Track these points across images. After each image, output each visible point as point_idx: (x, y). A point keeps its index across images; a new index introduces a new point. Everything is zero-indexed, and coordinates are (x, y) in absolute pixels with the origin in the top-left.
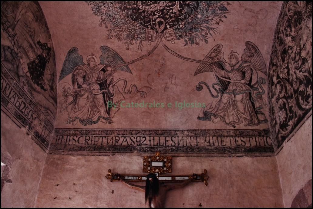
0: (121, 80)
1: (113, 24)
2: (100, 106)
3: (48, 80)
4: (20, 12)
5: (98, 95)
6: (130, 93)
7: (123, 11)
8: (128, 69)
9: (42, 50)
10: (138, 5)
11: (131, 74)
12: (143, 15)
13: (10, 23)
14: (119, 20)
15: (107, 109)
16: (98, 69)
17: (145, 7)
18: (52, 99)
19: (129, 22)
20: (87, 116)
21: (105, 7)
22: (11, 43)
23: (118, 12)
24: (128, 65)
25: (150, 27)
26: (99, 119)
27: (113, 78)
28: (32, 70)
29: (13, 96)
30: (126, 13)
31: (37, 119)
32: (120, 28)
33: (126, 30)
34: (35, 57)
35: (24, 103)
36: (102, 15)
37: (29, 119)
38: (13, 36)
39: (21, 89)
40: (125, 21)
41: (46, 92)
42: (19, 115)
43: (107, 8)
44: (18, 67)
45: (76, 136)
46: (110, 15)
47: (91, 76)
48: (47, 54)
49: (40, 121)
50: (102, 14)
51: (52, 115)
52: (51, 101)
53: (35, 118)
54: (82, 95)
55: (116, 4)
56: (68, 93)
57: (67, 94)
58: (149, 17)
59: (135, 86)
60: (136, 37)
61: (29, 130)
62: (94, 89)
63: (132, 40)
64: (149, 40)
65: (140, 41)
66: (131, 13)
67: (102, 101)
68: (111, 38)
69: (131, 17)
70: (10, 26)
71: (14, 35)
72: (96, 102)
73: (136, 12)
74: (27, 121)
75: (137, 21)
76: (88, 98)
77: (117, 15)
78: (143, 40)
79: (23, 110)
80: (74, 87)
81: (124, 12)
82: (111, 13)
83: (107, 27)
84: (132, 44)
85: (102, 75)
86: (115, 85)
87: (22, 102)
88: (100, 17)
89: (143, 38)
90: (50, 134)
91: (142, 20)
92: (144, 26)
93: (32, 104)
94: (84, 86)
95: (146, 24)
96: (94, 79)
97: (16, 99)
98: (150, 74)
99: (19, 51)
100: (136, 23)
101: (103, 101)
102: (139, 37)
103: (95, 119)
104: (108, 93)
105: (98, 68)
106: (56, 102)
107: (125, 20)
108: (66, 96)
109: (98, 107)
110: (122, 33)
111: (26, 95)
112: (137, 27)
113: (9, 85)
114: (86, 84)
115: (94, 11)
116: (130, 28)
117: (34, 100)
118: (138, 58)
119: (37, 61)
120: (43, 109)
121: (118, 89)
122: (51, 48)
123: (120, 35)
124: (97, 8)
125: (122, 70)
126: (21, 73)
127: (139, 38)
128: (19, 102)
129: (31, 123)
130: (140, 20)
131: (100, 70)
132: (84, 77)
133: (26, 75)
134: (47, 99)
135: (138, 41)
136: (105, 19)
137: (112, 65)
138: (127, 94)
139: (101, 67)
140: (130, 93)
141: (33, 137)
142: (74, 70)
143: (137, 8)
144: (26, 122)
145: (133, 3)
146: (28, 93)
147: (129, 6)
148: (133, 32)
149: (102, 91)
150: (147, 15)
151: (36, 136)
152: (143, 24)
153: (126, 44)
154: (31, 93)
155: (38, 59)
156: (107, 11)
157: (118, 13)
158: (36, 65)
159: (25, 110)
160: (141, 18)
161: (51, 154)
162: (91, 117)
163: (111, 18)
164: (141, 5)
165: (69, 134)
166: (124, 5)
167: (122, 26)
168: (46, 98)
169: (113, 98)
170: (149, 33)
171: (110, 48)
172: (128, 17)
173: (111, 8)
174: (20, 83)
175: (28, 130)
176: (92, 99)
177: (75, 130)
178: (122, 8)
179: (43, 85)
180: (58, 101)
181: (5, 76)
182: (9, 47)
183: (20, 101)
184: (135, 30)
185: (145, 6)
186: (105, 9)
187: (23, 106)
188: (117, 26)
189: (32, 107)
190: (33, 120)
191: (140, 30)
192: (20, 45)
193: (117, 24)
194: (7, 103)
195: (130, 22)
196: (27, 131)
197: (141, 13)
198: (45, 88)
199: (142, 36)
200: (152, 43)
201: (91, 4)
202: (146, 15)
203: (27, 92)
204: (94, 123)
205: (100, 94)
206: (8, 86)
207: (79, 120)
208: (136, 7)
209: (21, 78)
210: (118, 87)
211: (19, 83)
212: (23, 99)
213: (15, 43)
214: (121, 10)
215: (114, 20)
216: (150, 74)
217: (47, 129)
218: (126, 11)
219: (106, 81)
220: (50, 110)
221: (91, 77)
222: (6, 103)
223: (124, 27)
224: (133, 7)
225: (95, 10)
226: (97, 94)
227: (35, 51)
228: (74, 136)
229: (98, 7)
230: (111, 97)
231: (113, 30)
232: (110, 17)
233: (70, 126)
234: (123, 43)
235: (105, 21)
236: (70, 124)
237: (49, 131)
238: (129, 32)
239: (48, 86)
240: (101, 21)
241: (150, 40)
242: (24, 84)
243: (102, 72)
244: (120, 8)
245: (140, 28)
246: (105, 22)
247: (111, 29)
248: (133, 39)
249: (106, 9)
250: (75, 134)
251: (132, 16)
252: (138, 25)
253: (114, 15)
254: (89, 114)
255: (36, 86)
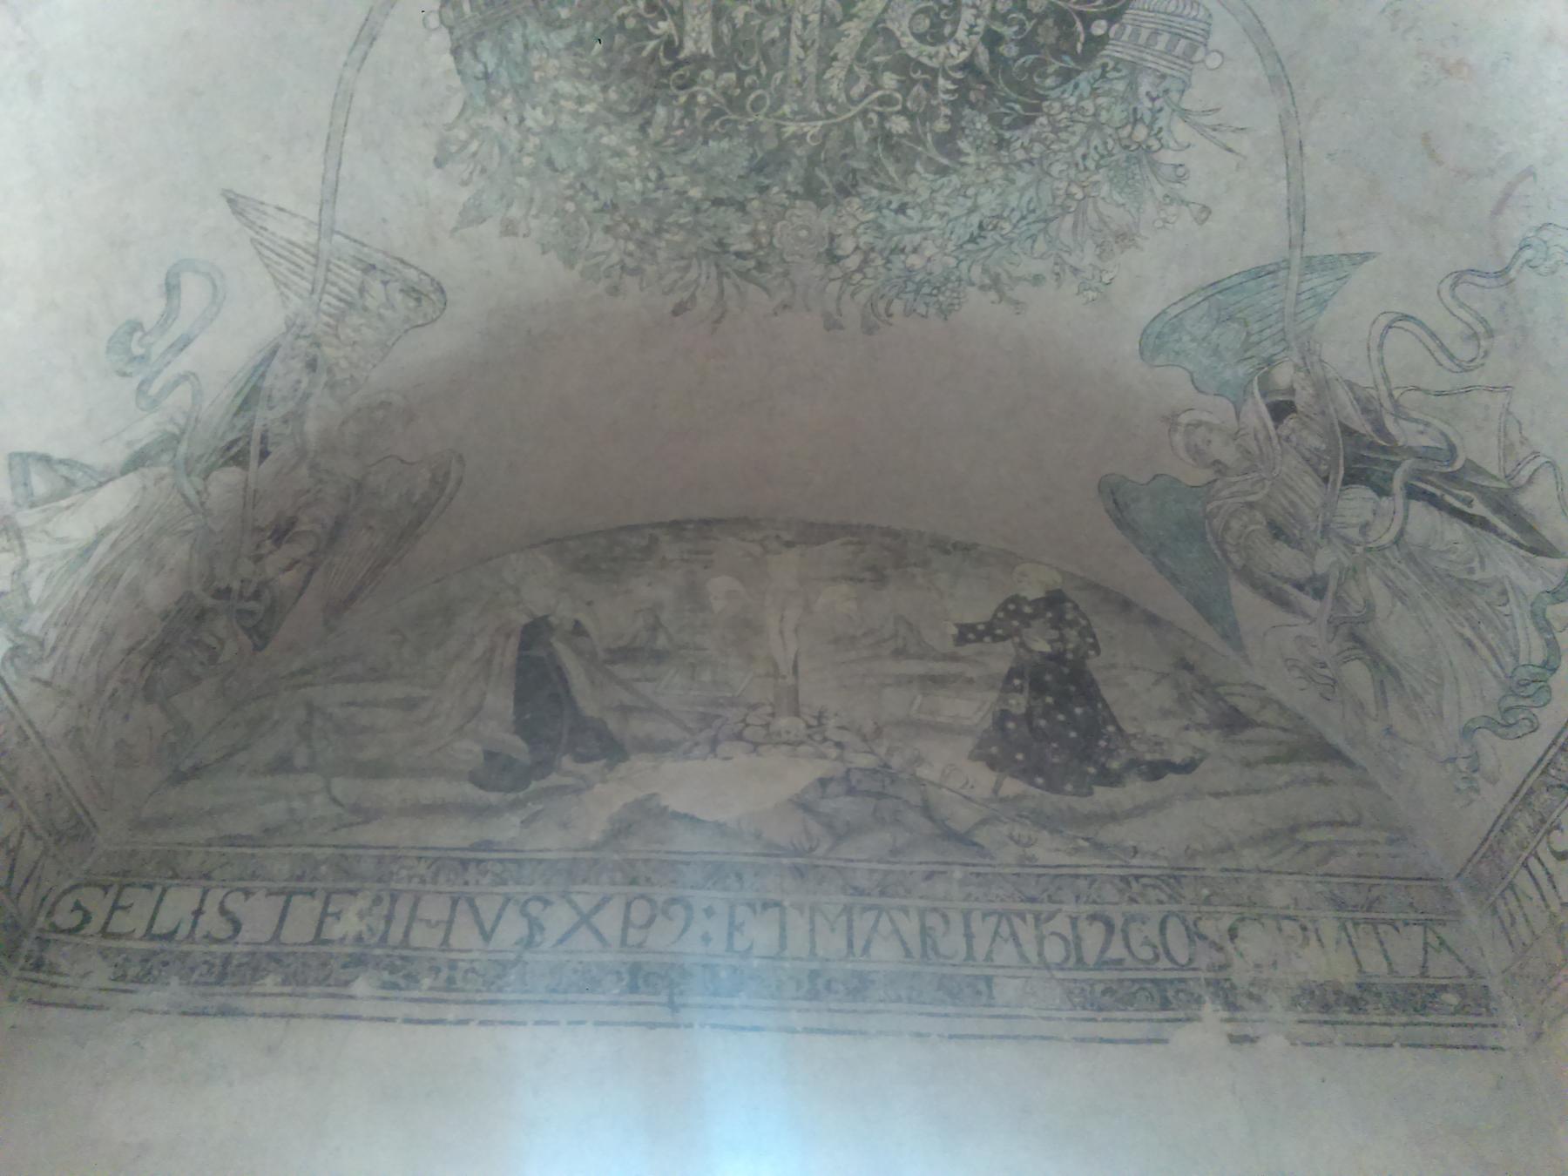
0: (1381, 346)
1: (1030, 241)
2: (1476, 564)
3: (1166, 714)
4: (781, 633)
5: (1409, 528)
6: (1490, 334)
7: (963, 164)
8: (1328, 263)
9: (1008, 643)
10: (942, 65)
11: (1371, 263)
12: (1009, 50)
13: (763, 704)
14: (1013, 201)
15: (1515, 535)
16: (1261, 436)
17: (963, 26)
18: (1279, 767)
19: (1038, 148)
20: (1495, 676)
21: (915, 251)
22: (823, 756)
23: (961, 191)
24: (1307, 252)
25: (1103, 23)
26: (1544, 627)
27: (1351, 386)
28: (1020, 757)
29: (996, 933)
30: (977, 148)
31: (1243, 931)
32: (1065, 210)
33: (1082, 177)
34: (993, 696)
35: (1093, 918)
36: (959, 280)
37: (1191, 960)
38: (809, 732)
39: (1018, 875)
40: (1027, 166)
41: (1204, 766)
42: (1104, 993)
43: (925, 244)
44: (927, 810)
45: (1558, 827)
46: (972, 240)
47: (1285, 496)
48: (1055, 627)
49: (1285, 924)
50: (953, 278)
51: (1356, 834)
52: (1285, 778)
53: (1233, 934)
54: (1369, 606)
55: (911, 187)
56: (1324, 666)
57: (1326, 672)
58: (1037, 15)
59: (1458, 277)
60: (1141, 132)
61: (1239, 1015)
62: (1365, 528)
63: (1154, 166)
64: (1188, 57)
65: (1176, 118)
66: (985, 119)
67: (1456, 531)
68: (1106, 279)
69: (1010, 127)
70: (773, 715)
71: (814, 722)
72: (1443, 566)
73: (983, 87)
74: (1182, 980)
75: (1044, 98)
76: (1400, 595)
77: (981, 200)
78: (1175, 96)
79: (1117, 950)
80: (1305, 615)
81: (971, 160)
82: (960, 231)
83: (1037, 279)
84: (1180, 174)
85: (1305, 433)
86: (1396, 393)
87: (1074, 921)
88: (972, 291)
89: (1166, 91)
90: (1442, 931)
91: (1043, 63)
92: (1086, 58)
93: (1145, 886)
94: (1326, 560)
95: (1079, 47)
96: (1308, 485)
97: (1026, 932)
98: (1426, 138)
99: (882, 751)
100: (1057, 105)
101: (1456, 526)
102: (1147, 119)
103: (1533, 649)
104: (1423, 466)
105: (1255, 436)
106: (1331, 754)
107: (1019, 165)
108: (1333, 687)
109: (1476, 577)
110: (1096, 209)
111: (1077, 876)
112: (1080, 110)
113: (935, 910)
114: (1318, 545)
115: (932, 311)
116: (1080, 151)
117: (1148, 861)
118: (1282, 170)
119: (1018, 703)
120: (1249, 858)
121: (1427, 392)
122: (1059, 591)
123: (1105, 223)
124: (917, 291)
125: (1322, 304)
126: (963, 817)
127: (1154, 119)
128: (1053, 933)
129: (1221, 975)
130: (1044, 76)
131: (1270, 424)
132: (1277, 532)
133: (1003, 800)
134: (1238, 793)
135: (1170, 131)
136: (985, 271)
137: (1268, 349)
138: (1486, 354)
139: (1257, 412)
140: (1490, 334)
141: (1302, 1029)
142: (1218, 552)
143: (959, 75)
144: (1178, 992)
145: (924, 93)
146: (1075, 860)
147: (937, 117)
148: (1105, 143)
149: (1397, 485)
150: (1022, 25)
151: (1326, 1008)
152: (1072, 65)
153: (1172, 209)
154: (1099, 847)
155: (1020, 690)
156: (942, 248)
157: (971, 192)
158: (1028, 716)
159: (1128, 946)
160: (1031, 70)
161: (1539, 1035)
162: (1509, 659)
163: (992, 236)
164: (942, 49)
165: (1523, 848)
166: (924, 144)
167: (1054, 197)
168: (1226, 794)
169: (1468, 460)
170: (1142, 40)
171: (1164, 312)
172: (1002, 143)
173: (933, 221)
174: (992, 858)
175: (1229, 1020)
176: (1413, 577)
177: (1526, 802)
178: (945, 161)
179: (1148, 757)
180: (1337, 739)
181: (882, 894)
182: (823, 782)
183: (1061, 924)
184: (1095, 125)
185: (956, 23)
186: (928, 253)
187: (1093, 936)
188: (1047, 221)
189: (1161, 902)
190: (1220, 949)
191: (1108, 93)
192: (869, 727)
193: (1031, 218)
194: (982, 986)
195: (1042, 141)
196: (1228, 1028)
197: (995, 58)
198: (1179, 755)
199: (1148, 94)
200: (1215, 40)
201: (887, 310)
202: (1016, 33)
203: (1067, 860)
204: (1554, 670)
205: (1407, 509)
206: (933, 920)
207: (1486, 732)
208: (954, 81)
209: (982, 836)
210: (1418, 389)
211: (987, 861)
212: (1070, 908)
213: (839, 745)
214: (956, 171)
215: (1007, 227)
216: (1426, 138)
217: (1392, 923)
218: (963, 145)
219: (1348, 432)
220: (1314, 825)
221: (1292, 496)
222: (979, 993)
223: (1063, 185)
224: (946, 97)
225: (927, 305)
226: (1395, 530)
227: (970, 681)
228: (1548, 832)
229: (911, 286)
230: (1458, 465)
231: (1065, 256)
232: (983, 244)
233: (1493, 799)
234: (1159, 224)
235: (998, 275)
236: (1477, 791)
237: (1424, 924)
238: (1098, 167)
239: (1195, 737)
240: (993, 295)
241: (1194, 49)
242: (1017, 842)
243: (1290, 422)
244: (943, 171)
245: (1094, 93)
246: (1004, 277)
247: (1056, 264)
248: (1155, 156)
249: (930, 249)
250: (1543, 821)
251: (1007, 120)
252: (1072, 101)
253: (975, 219)
254: (1485, 652)
255: (1103, 795)
